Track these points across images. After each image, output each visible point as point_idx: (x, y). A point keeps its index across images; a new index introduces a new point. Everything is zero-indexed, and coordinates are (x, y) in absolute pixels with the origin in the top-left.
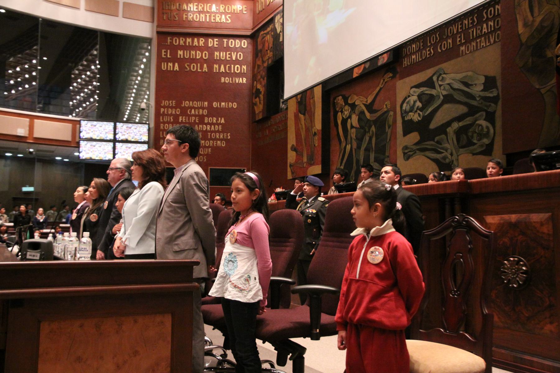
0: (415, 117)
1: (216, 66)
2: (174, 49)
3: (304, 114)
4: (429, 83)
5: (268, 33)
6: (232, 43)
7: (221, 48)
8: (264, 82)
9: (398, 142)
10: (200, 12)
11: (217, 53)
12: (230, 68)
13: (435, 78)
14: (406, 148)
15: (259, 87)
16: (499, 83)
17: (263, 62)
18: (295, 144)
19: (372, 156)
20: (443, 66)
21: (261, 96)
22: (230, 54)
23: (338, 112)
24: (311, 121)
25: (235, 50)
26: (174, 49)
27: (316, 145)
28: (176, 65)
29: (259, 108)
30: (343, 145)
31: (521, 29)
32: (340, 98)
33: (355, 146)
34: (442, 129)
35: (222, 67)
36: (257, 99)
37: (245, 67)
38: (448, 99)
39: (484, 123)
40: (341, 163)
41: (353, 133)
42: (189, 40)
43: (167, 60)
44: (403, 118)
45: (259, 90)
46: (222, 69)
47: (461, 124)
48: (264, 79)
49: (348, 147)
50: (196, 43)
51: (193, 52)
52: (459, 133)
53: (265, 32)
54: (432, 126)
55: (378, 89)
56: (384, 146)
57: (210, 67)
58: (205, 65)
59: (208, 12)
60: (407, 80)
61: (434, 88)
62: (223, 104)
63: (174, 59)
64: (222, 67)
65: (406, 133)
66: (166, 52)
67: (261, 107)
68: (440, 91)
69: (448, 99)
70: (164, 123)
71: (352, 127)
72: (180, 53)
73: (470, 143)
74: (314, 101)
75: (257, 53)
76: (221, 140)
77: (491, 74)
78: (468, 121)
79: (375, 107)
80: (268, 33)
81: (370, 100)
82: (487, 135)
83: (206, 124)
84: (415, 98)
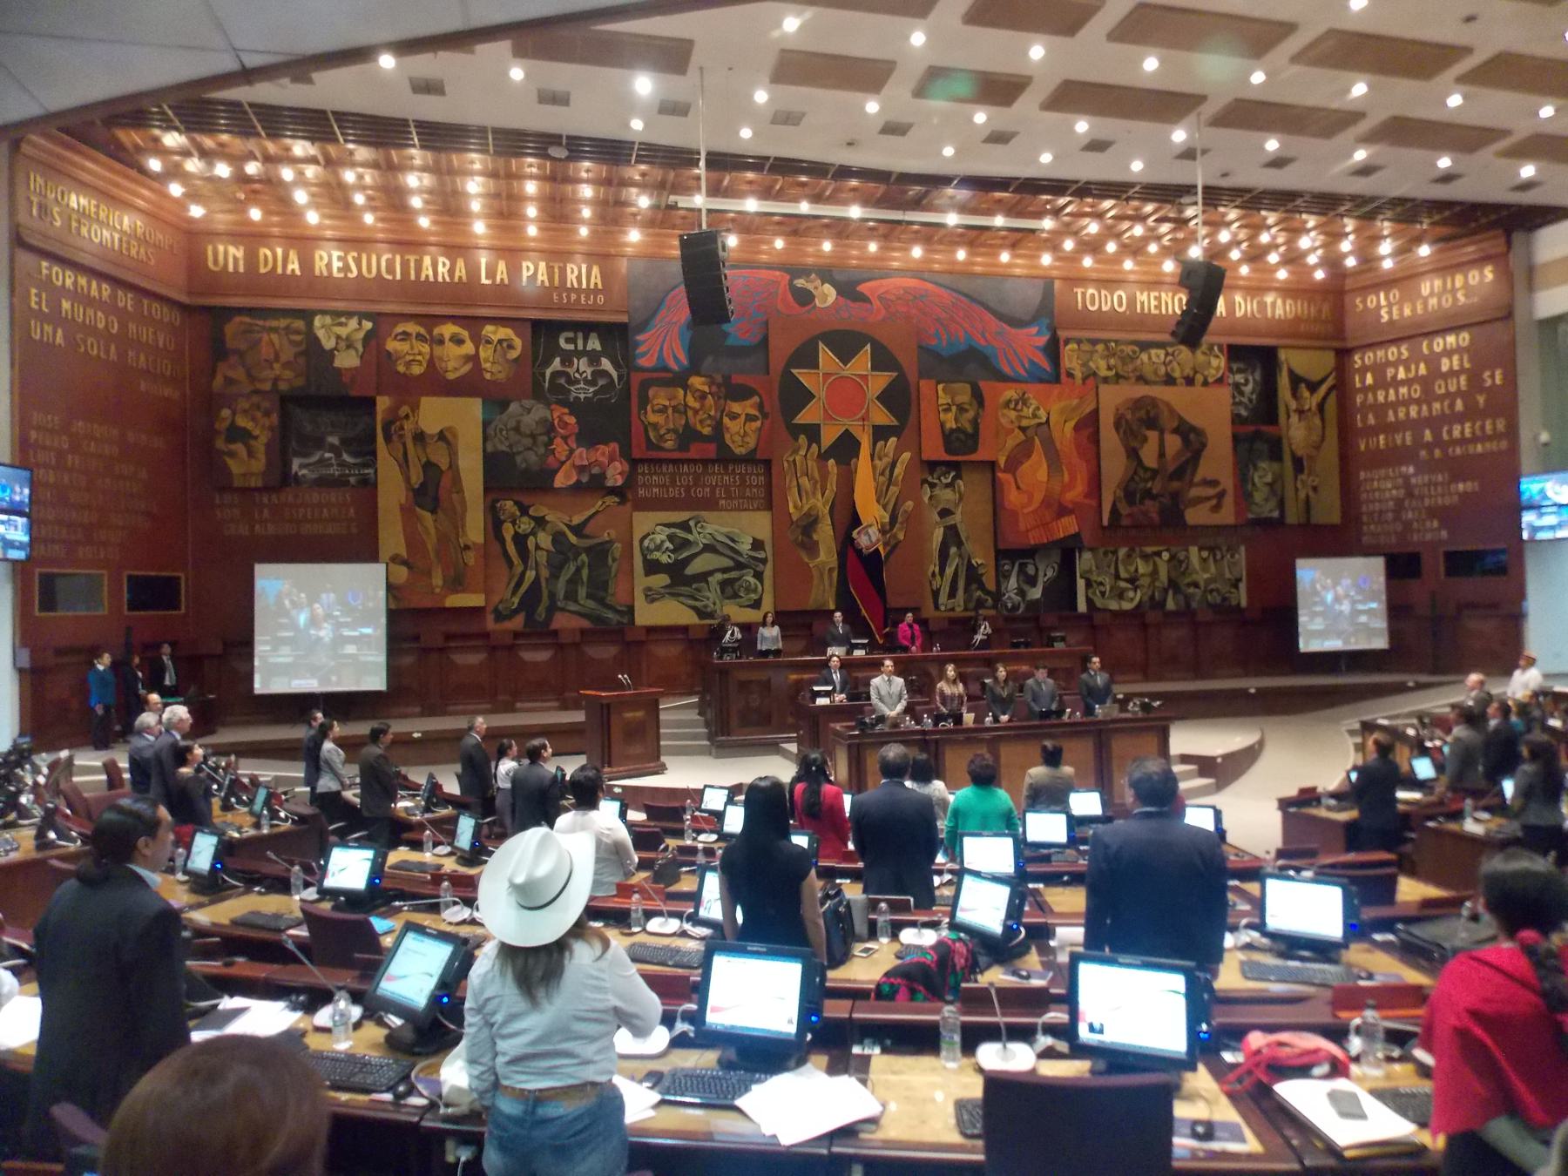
0: (664, 559)
3: (433, 512)
4: (684, 526)
9: (636, 582)
11: (132, 327)
13: (692, 523)
14: (649, 589)
15: (242, 422)
16: (768, 547)
17: (252, 378)
18: (404, 554)
19: (582, 592)
20: (703, 513)
21: (260, 446)
23: (502, 522)
24: (456, 528)
27: (471, 562)
28: (60, 332)
29: (248, 465)
30: (519, 568)
31: (792, 510)
32: (509, 503)
33: (545, 573)
34: (703, 577)
38: (708, 548)
39: (752, 580)
40: (514, 593)
41: (542, 557)
44: (644, 557)
45: (244, 429)
47: (726, 576)
48: (267, 414)
49: (530, 575)
50: (94, 292)
52: (724, 584)
53: (261, 323)
54: (689, 571)
55: (593, 511)
56: (607, 582)
58: (113, 348)
60: (651, 515)
61: (690, 532)
63: (55, 317)
65: (647, 574)
67: (259, 464)
68: (698, 537)
69: (708, 548)
71: (538, 547)
72: (66, 305)
73: (736, 596)
74: (463, 502)
77: (759, 537)
78: (733, 574)
79: (587, 531)
80: (275, 330)
81: (576, 520)
82: (755, 591)
84: (664, 537)
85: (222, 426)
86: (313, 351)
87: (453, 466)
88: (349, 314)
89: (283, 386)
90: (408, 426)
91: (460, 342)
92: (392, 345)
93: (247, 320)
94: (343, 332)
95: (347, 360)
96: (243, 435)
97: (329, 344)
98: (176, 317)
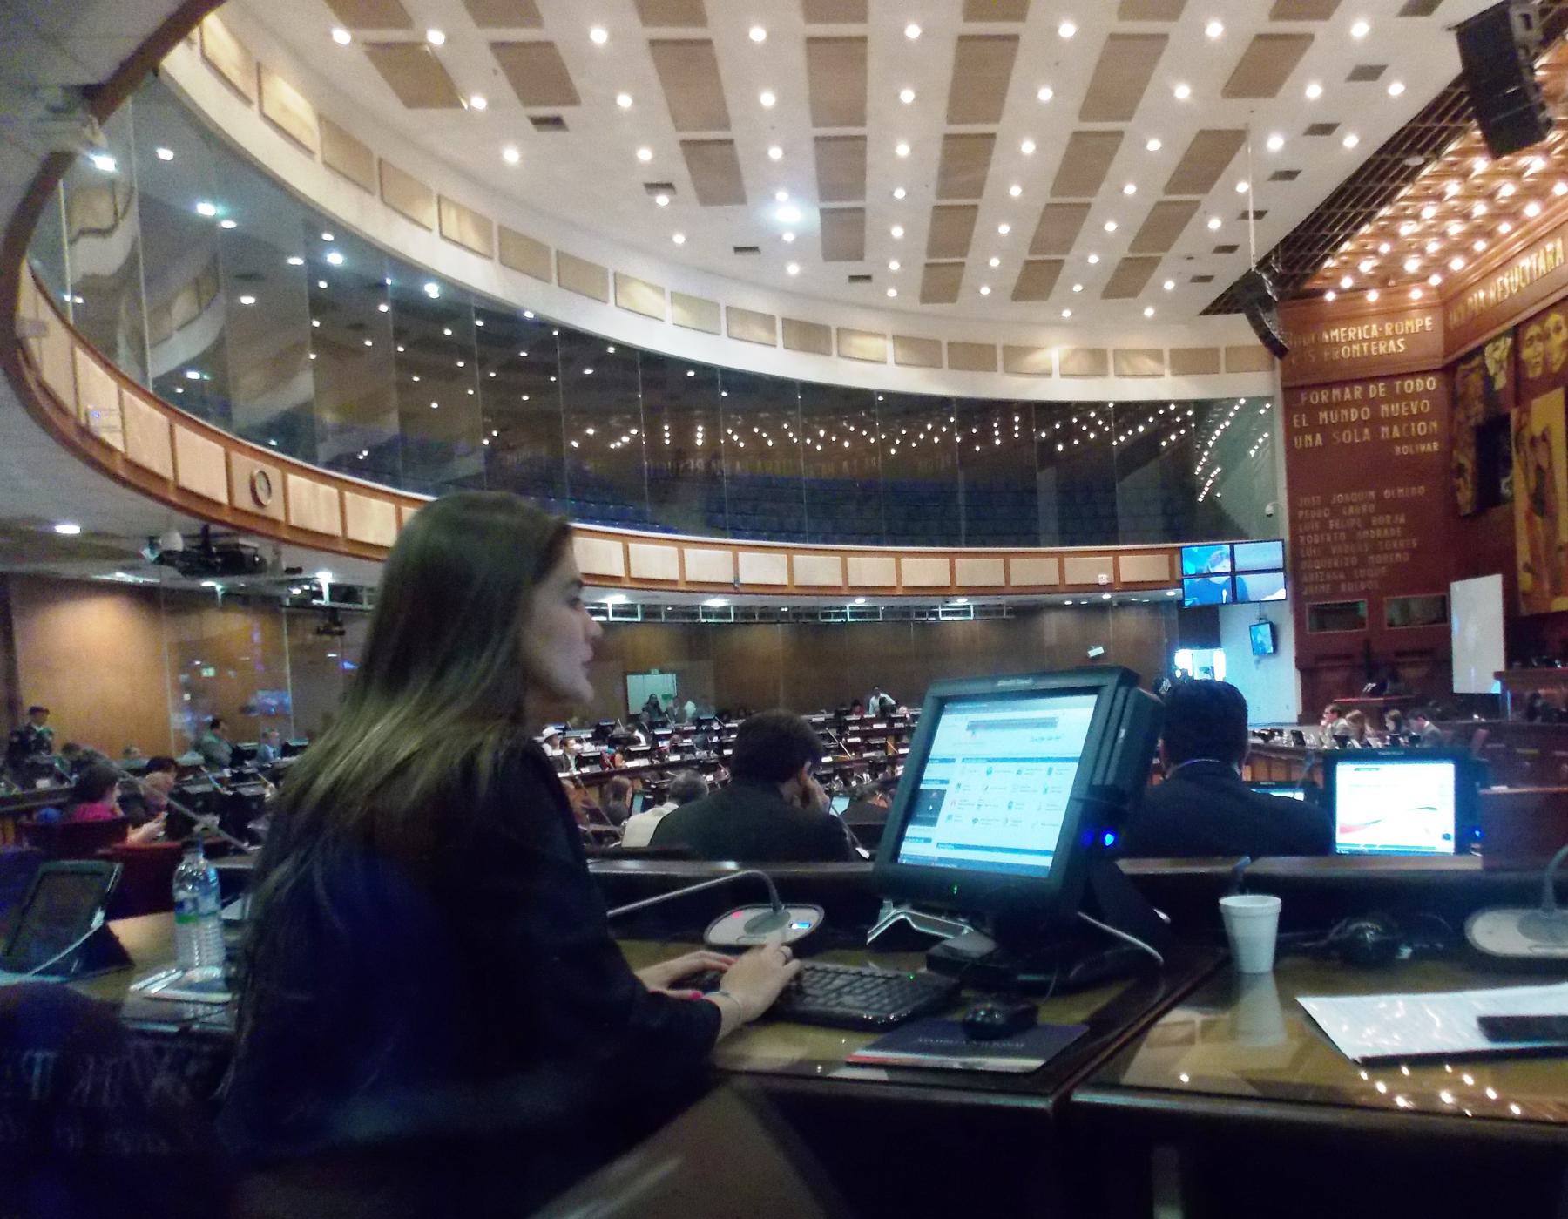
1: (1385, 429)
2: (1312, 411)
5: (1472, 370)
6: (1411, 385)
7: (1392, 397)
8: (1472, 453)
10: (1350, 343)
11: (1384, 408)
12: (1409, 429)
15: (1463, 460)
17: (1468, 418)
22: (1408, 405)
25: (1417, 396)
26: (1312, 411)
29: (1466, 495)
35: (1395, 428)
36: (1461, 481)
37: (1434, 424)
42: (1336, 392)
43: (1302, 431)
46: (1396, 433)
50: (1348, 396)
51: (1344, 412)
57: (1375, 433)
58: (1366, 431)
59: (1364, 340)
62: (1401, 491)
63: (1314, 427)
64: (1395, 428)
66: (1300, 418)
70: (1306, 534)
72: (1323, 415)
75: (1454, 399)
76: (1401, 551)
80: (1472, 370)
83: (1375, 528)
85: (1454, 465)
86: (1488, 380)
87: (1551, 464)
88: (1498, 338)
89: (1480, 419)
90: (1526, 434)
91: (1558, 329)
92: (1527, 353)
93: (1463, 367)
94: (1497, 355)
95: (1501, 382)
96: (1460, 470)
97: (1492, 372)
98: (1431, 383)
